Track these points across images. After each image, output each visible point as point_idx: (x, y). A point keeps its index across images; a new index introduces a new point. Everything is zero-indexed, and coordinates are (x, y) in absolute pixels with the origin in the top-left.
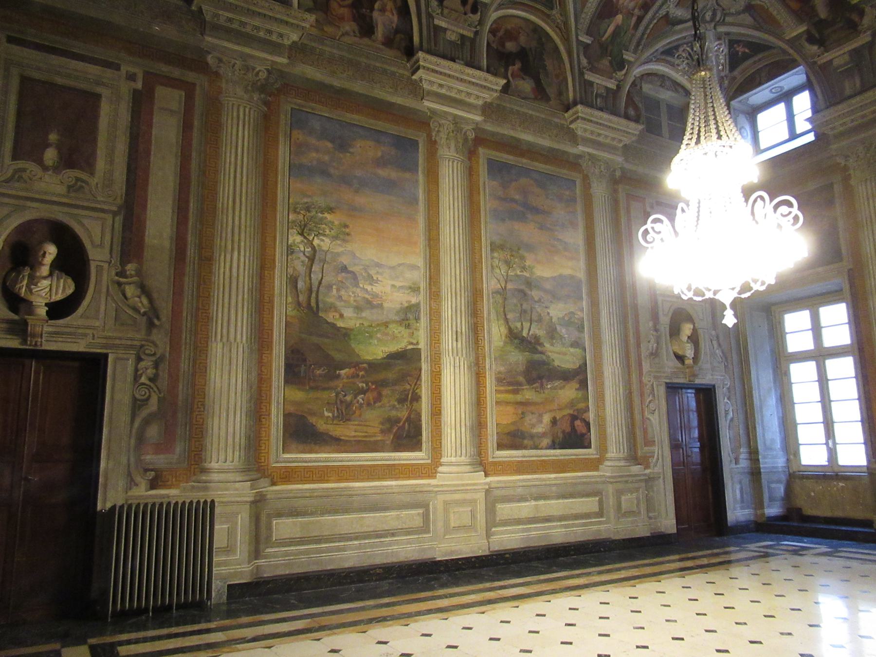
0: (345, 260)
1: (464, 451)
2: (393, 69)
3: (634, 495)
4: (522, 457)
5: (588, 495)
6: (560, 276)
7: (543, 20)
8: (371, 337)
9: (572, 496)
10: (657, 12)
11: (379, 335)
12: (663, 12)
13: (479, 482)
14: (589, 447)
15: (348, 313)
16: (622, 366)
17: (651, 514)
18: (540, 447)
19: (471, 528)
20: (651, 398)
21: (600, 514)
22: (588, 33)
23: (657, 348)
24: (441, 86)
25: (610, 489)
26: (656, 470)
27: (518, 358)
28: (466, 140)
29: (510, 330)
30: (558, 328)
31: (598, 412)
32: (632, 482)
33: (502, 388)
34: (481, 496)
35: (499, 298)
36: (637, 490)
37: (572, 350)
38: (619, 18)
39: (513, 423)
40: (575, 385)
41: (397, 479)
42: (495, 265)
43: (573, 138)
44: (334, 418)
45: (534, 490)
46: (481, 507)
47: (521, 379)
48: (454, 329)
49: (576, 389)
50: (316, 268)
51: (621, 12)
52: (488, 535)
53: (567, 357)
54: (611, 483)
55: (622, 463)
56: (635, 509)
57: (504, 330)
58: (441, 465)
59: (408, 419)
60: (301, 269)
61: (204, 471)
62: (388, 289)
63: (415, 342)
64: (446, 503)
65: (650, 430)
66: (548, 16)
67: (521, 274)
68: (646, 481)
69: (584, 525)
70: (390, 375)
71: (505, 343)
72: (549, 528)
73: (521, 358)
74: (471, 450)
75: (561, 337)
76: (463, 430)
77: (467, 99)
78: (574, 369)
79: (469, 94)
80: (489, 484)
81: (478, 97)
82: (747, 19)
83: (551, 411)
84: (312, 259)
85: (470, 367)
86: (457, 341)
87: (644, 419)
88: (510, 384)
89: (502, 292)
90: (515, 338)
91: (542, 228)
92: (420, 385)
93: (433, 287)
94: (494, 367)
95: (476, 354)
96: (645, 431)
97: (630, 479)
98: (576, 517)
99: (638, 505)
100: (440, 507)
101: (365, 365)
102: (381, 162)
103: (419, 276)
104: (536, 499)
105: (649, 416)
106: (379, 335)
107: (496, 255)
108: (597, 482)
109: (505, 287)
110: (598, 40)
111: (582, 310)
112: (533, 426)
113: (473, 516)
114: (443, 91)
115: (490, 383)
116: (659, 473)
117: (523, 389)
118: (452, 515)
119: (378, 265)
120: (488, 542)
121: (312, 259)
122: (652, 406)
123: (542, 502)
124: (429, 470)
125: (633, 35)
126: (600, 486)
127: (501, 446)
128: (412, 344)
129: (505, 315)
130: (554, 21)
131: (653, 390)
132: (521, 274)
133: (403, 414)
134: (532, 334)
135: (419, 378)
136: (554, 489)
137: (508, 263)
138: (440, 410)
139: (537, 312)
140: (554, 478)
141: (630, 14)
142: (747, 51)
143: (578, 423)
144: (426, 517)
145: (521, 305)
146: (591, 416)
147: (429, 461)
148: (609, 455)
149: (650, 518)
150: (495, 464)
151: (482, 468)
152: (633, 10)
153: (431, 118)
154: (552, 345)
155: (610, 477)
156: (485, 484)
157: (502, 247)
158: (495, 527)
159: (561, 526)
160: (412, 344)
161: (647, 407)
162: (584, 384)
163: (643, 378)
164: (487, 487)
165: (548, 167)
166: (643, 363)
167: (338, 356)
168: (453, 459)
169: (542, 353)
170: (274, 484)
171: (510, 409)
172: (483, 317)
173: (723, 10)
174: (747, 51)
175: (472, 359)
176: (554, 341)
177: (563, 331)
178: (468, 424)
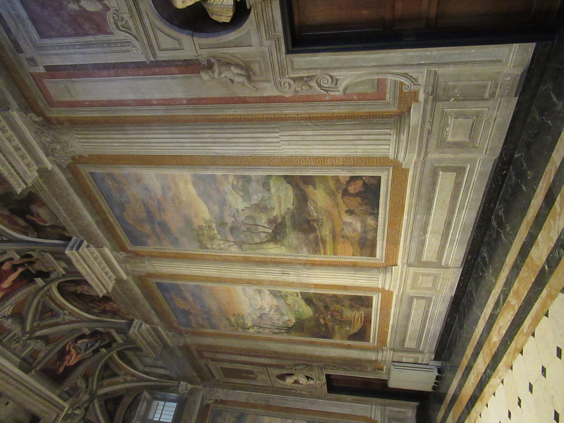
0: (255, 317)
1: (376, 276)
2: (120, 291)
3: (451, 121)
4: (383, 241)
5: (434, 184)
6: (201, 195)
8: (298, 311)
9: (430, 201)
11: (296, 308)
13: (400, 271)
14: (379, 179)
15: (286, 318)
16: (277, 130)
17: (487, 95)
18: (375, 226)
19: (436, 278)
20: (313, 84)
21: (459, 171)
23: (237, 66)
24: (106, 273)
25: (433, 156)
26: (422, 80)
27: (293, 237)
28: (130, 257)
29: (269, 241)
30: (253, 202)
31: (338, 166)
32: (432, 124)
33: (322, 251)
34: (412, 270)
35: (245, 247)
36: (444, 115)
37: (273, 190)
39: (352, 245)
40: (310, 190)
41: (390, 308)
42: (218, 248)
43: (43, 172)
44: (350, 327)
45: (416, 234)
46: (422, 270)
47: (311, 236)
48: (281, 275)
49: (315, 189)
50: (265, 326)
52: (447, 267)
53: (282, 195)
54: (426, 154)
55: (404, 137)
56: (470, 121)
57: (271, 245)
58: (384, 288)
59: (349, 300)
60: (267, 331)
61: (376, 360)
62: (263, 302)
63: (296, 294)
64: (413, 288)
65: (360, 89)
67: (215, 229)
68: (436, 99)
69: (466, 191)
70: (321, 305)
71: (282, 245)
72: (457, 224)
73: (292, 236)
74: (375, 272)
75: (263, 199)
76: (357, 275)
77: (99, 256)
78: (293, 188)
79: (96, 259)
80: (403, 264)
81: (92, 254)
83: (340, 214)
84: (260, 327)
85: (308, 269)
86: (289, 274)
87: (346, 99)
88: (317, 245)
89: (240, 244)
90: (276, 238)
91: (161, 209)
92: (325, 294)
93: (254, 283)
94: (304, 255)
95: (296, 264)
96: (363, 97)
97: (428, 126)
98: (454, 197)
99: (465, 116)
100: (414, 291)
101: (316, 315)
102: (185, 299)
103: (250, 290)
104: (425, 232)
105: (341, 89)
106: (296, 308)
107: (209, 246)
108: (422, 173)
109: (233, 242)
111: (226, 176)
112: (355, 230)
113: (429, 275)
114: (108, 269)
115: (318, 258)
116: (429, 73)
117: (321, 236)
118: (423, 286)
119: (251, 305)
120: (452, 268)
121: (260, 327)
122: (326, 83)
123: (430, 228)
124: (387, 296)
126: (428, 168)
127: (372, 254)
128: (297, 295)
129: (258, 244)
131: (301, 78)
132: (215, 229)
133: (347, 303)
134: (268, 225)
135: (321, 294)
136: (418, 217)
137: (212, 239)
138: (343, 286)
139: (245, 219)
140: (408, 216)
143: (351, 189)
144: (418, 298)
145: (244, 231)
146: (344, 174)
147: (380, 294)
148: (391, 156)
149: (492, 95)
150: (386, 259)
151: (390, 268)
153: (133, 275)
154: (274, 209)
155: (419, 155)
156: (403, 266)
157: (200, 242)
158: (441, 262)
159: (459, 213)
160: (297, 295)
161: (327, 91)
162: (308, 180)
163: (287, 96)
164: (405, 265)
165: (98, 198)
166: (266, 95)
167: (312, 323)
168: (380, 282)
169: (283, 218)
170: (386, 346)
171: (339, 246)
172: (265, 258)
175: (302, 267)
176: (269, 207)
177: (256, 199)
178: (353, 273)
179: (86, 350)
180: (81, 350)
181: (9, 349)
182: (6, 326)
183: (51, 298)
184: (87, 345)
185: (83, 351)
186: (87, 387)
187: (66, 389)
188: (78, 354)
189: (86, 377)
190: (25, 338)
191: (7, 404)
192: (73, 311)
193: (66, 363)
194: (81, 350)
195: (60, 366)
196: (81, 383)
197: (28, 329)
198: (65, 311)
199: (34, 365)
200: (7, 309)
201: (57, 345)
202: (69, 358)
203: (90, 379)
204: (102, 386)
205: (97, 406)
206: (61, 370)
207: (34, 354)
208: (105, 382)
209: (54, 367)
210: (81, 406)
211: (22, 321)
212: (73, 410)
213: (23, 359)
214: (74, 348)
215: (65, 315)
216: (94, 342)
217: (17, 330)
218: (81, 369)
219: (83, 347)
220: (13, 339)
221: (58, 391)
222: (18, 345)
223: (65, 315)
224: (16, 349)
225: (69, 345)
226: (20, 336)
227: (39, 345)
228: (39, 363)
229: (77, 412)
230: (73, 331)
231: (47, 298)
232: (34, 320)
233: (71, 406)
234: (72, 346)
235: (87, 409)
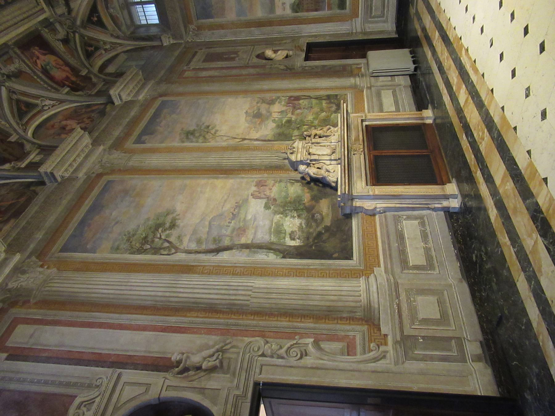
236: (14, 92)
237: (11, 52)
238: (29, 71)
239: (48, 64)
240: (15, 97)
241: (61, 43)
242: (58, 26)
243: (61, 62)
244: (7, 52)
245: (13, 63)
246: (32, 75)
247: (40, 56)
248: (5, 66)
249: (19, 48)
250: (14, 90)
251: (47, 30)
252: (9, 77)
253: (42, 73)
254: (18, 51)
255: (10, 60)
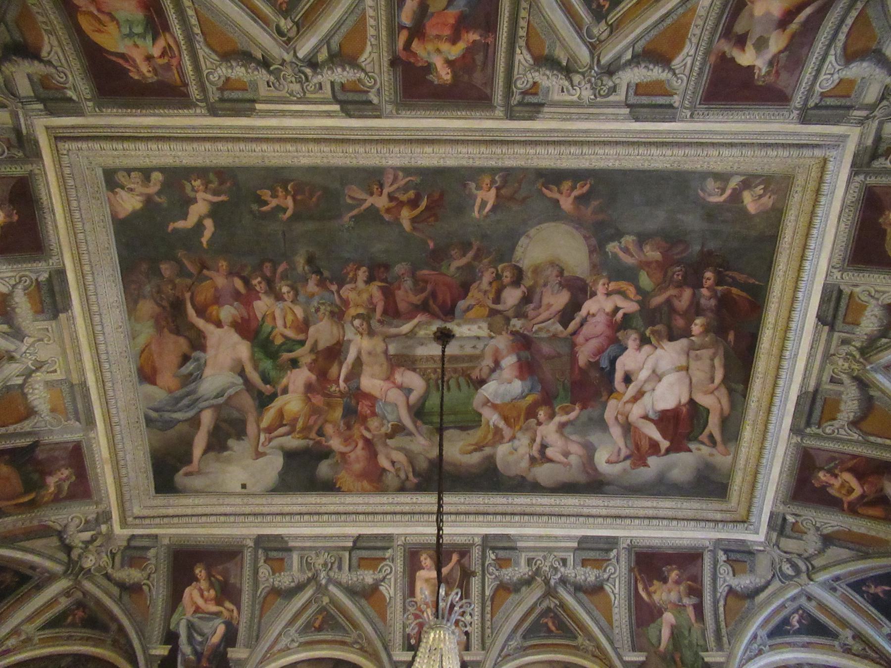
7: (576, 655)
10: (715, 589)
12: (722, 590)
22: (634, 649)
38: (669, 617)
51: (666, 610)
66: (576, 648)
82: (834, 552)
110: (655, 652)
125: (703, 632)
130: (587, 651)
141: (679, 607)
142: (887, 588)
152: (680, 600)
173: (800, 555)
174: (887, 588)
179: (191, 626)
180: (199, 618)
181: (328, 550)
182: (366, 572)
183: (343, 643)
184: (202, 634)
185: (195, 620)
186: (108, 577)
187: (151, 553)
188: (197, 610)
189: (131, 590)
190: (322, 576)
191: (244, 486)
192: (291, 654)
193: (204, 584)
194: (199, 618)
195: (209, 576)
196: (133, 575)
197: (332, 588)
198: (296, 644)
199: (260, 551)
200: (392, 592)
201: (254, 596)
202: (206, 593)
203: (115, 591)
204: (67, 593)
205: (48, 564)
206: (200, 571)
207: (278, 565)
208: (64, 603)
209: (220, 568)
210: (87, 547)
211: (352, 592)
212: (100, 533)
213: (290, 550)
214: (218, 614)
215: (293, 640)
216: (198, 648)
217: (345, 577)
218: (159, 593)
219: (206, 627)
220: (336, 565)
221: (166, 541)
222: (321, 561)
223: (293, 640)
224: (317, 555)
225: (233, 610)
226: (332, 574)
227: (285, 580)
228: (256, 560)
229: (87, 535)
230: (256, 638)
231: (348, 640)
232: (333, 601)
233: (110, 536)
234: (226, 613)
235: (68, 549)
236: (280, 33)
237: (214, 95)
238: (203, 51)
239: (131, 35)
240: (285, 24)
241: (44, 54)
242: (24, 88)
243: (85, 24)
244: (222, 100)
245: (228, 79)
246: (200, 38)
247: (139, 60)
248: (255, 86)
249: (186, 95)
250: (276, 35)
251: (70, 93)
252: (265, 63)
253: (166, 28)
254: (194, 91)
255: (227, 84)
